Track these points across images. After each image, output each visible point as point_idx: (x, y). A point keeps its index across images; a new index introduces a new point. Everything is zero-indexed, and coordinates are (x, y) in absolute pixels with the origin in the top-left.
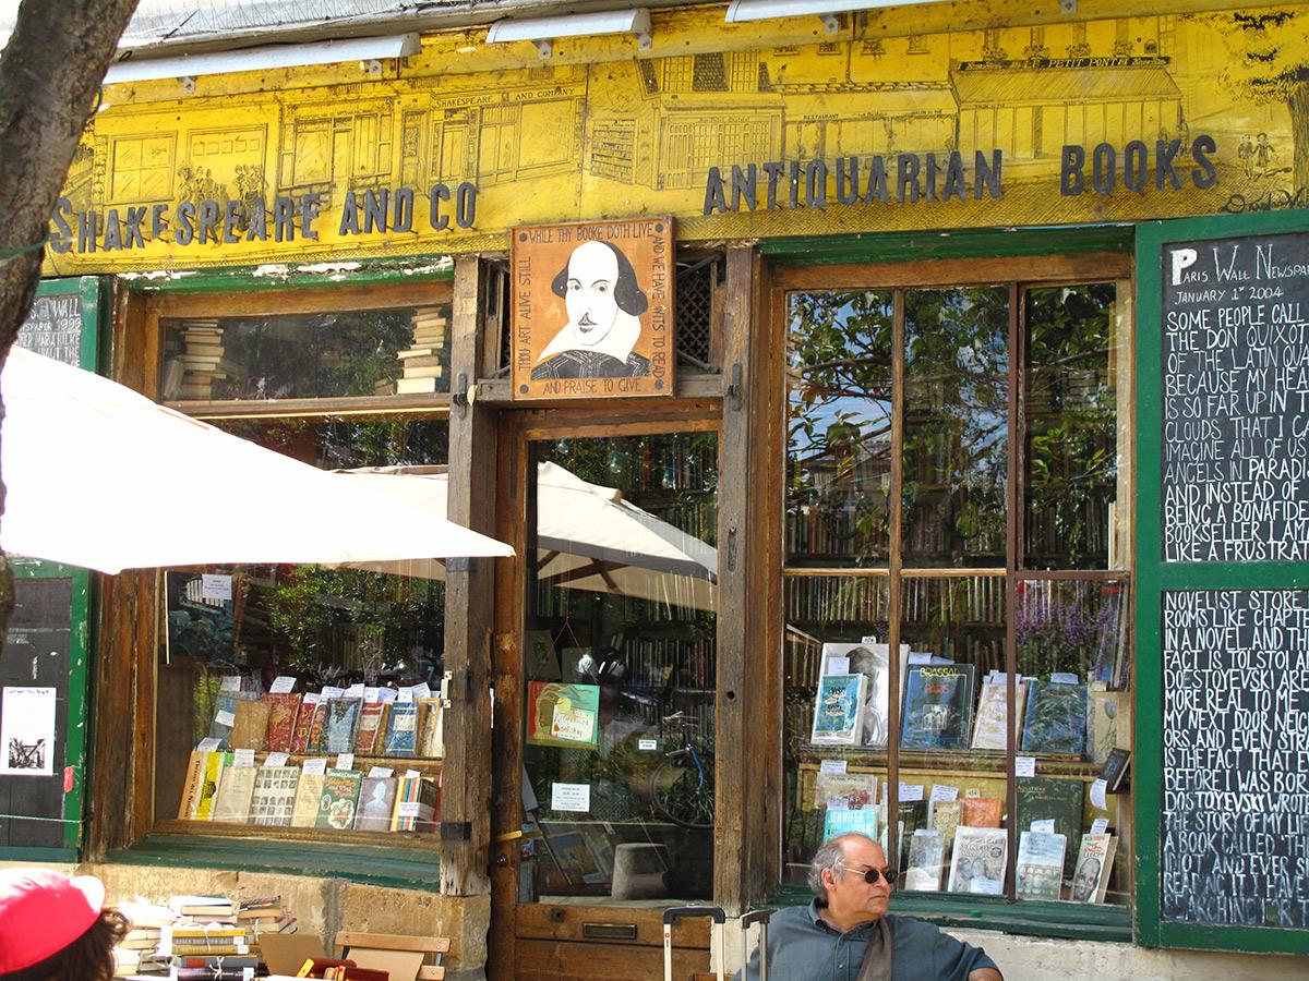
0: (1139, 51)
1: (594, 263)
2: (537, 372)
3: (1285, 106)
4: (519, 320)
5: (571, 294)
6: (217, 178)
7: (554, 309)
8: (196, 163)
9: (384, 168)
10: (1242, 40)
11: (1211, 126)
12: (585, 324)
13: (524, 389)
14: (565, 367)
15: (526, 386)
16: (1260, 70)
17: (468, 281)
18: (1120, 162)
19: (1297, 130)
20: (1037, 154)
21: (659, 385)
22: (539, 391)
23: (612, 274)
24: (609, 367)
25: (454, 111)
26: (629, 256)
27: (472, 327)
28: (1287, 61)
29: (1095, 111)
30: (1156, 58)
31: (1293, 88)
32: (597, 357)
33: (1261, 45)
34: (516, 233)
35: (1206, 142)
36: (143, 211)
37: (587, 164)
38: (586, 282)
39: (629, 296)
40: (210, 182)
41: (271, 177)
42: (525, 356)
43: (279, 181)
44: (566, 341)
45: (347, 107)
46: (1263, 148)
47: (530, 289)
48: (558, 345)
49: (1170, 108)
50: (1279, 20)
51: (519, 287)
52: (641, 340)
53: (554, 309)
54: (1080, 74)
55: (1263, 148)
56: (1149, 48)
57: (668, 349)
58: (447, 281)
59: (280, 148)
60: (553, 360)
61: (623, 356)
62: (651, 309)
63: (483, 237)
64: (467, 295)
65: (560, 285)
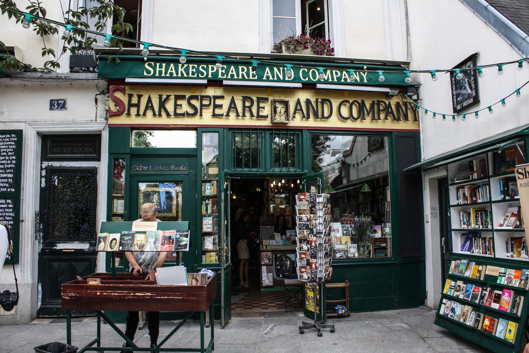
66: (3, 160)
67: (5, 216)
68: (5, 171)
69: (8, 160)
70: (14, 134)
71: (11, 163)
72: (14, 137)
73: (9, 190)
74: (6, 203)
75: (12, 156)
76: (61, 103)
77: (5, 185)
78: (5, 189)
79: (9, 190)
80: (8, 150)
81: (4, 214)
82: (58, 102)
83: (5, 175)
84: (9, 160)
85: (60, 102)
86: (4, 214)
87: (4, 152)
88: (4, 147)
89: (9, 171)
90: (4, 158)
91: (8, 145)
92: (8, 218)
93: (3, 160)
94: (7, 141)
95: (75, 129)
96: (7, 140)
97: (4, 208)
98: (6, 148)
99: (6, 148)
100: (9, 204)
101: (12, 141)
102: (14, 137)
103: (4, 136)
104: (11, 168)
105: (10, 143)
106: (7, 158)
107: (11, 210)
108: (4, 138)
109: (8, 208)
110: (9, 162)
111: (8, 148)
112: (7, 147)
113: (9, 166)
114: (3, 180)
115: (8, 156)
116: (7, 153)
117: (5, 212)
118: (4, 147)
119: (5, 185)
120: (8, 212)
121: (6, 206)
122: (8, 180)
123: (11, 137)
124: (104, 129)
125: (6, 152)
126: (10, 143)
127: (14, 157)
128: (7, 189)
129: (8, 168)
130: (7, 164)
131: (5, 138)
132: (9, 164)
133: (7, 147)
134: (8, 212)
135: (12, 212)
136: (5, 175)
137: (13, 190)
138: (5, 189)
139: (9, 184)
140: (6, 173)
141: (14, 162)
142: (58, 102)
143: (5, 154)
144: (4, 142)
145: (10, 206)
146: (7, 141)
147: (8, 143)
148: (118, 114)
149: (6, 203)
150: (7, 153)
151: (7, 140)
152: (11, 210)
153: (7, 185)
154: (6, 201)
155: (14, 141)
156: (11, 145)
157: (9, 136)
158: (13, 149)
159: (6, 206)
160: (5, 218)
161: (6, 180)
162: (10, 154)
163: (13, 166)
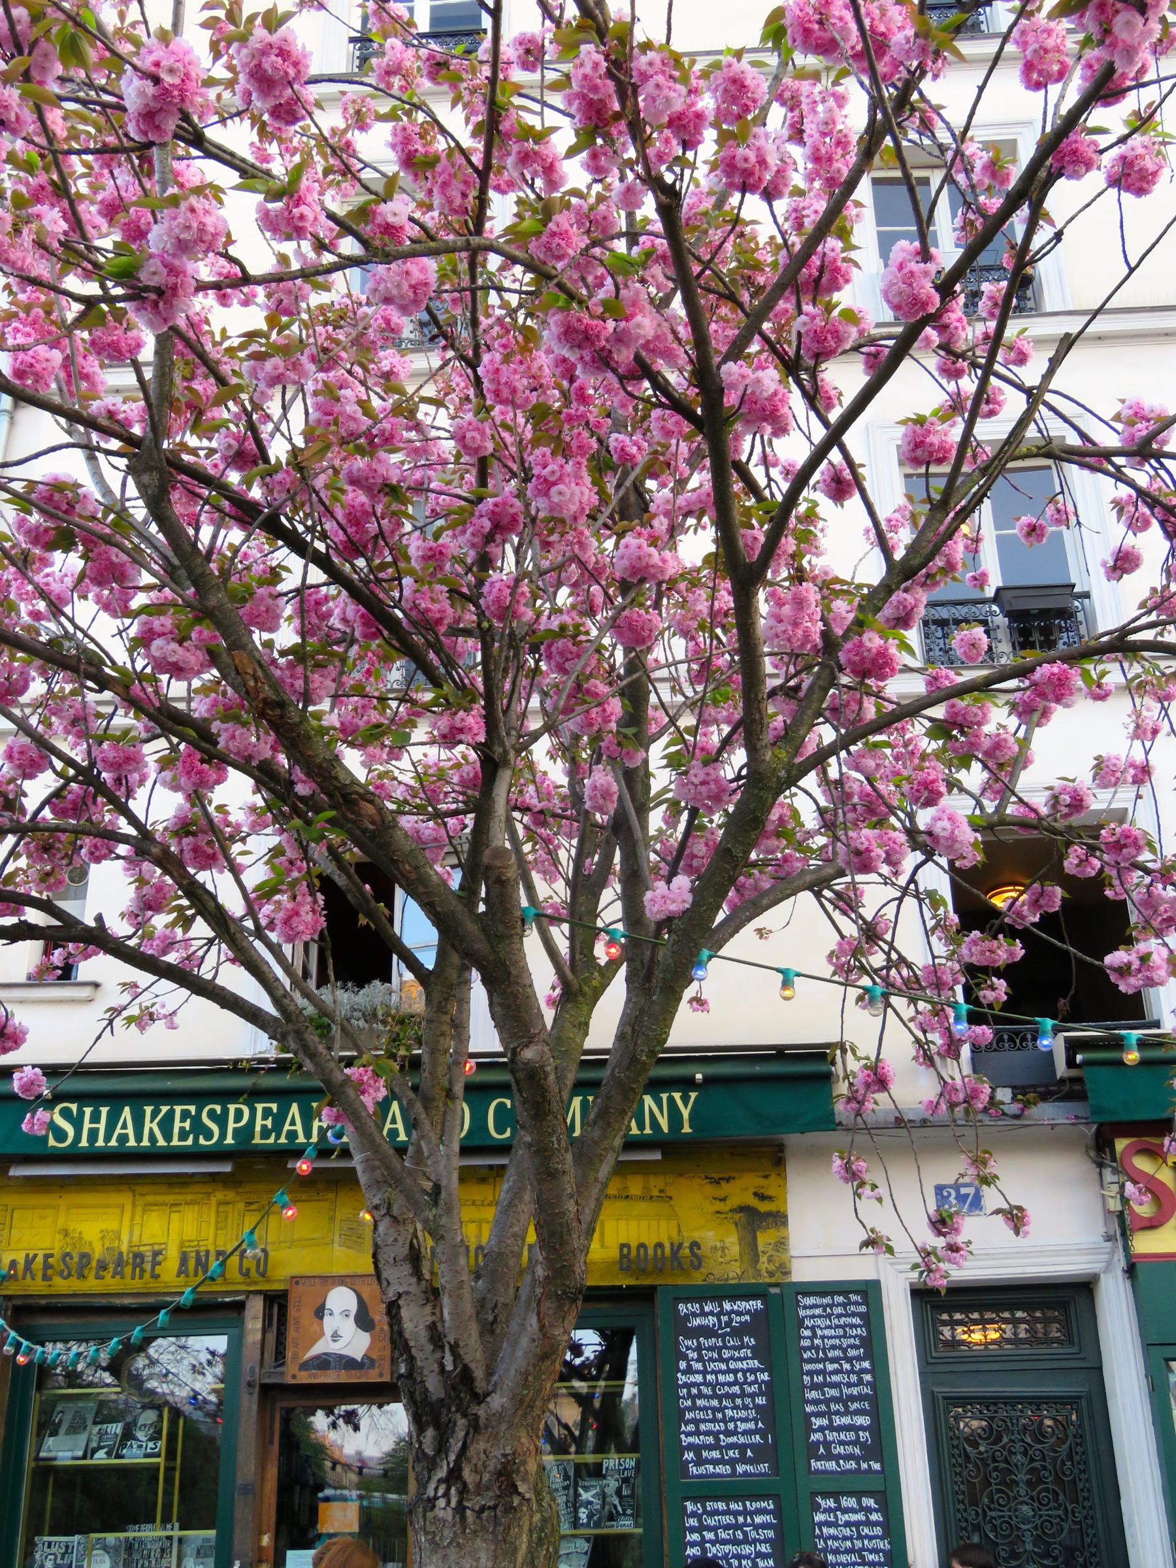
0: (655, 1193)
1: (341, 1300)
2: (304, 1366)
3: (733, 1227)
4: (291, 1333)
5: (327, 1319)
6: (87, 1236)
7: (316, 1327)
8: (72, 1226)
9: (203, 1236)
10: (710, 1190)
11: (697, 1236)
12: (336, 1336)
13: (294, 1377)
14: (323, 1362)
15: (294, 1375)
16: (720, 1206)
17: (256, 1307)
18: (651, 1252)
19: (741, 1239)
20: (602, 1246)
21: (381, 1375)
22: (304, 1378)
23: (353, 1306)
24: (349, 1363)
25: (250, 1203)
26: (364, 1296)
27: (259, 1336)
28: (733, 1202)
29: (633, 1223)
30: (665, 1198)
31: (737, 1216)
32: (341, 1357)
33: (720, 1193)
34: (296, 1280)
35: (695, 1245)
36: (35, 1256)
37: (337, 1238)
38: (336, 1312)
39: (363, 1320)
40: (81, 1238)
41: (125, 1238)
42: (295, 1356)
43: (130, 1241)
44: (322, 1347)
45: (179, 1197)
46: (723, 1248)
47: (298, 1313)
48: (318, 1349)
49: (673, 1224)
50: (728, 1180)
51: (292, 1312)
52: (370, 1348)
53: (316, 1327)
54: (624, 1203)
55: (723, 1248)
56: (661, 1191)
57: (387, 1353)
58: (239, 1307)
59: (132, 1219)
60: (317, 1357)
61: (358, 1357)
62: (377, 1328)
63: (269, 1281)
64: (255, 1318)
65: (320, 1312)
66: (836, 1372)
67: (863, 1549)
68: (846, 1407)
69: (848, 1373)
70: (856, 1292)
71: (860, 1382)
72: (856, 1303)
73: (864, 1466)
74: (862, 1509)
75: (859, 1359)
76: (968, 1195)
77: (849, 1449)
78: (852, 1465)
79: (864, 1466)
80: (845, 1342)
81: (858, 1544)
82: (958, 1192)
83: (846, 1420)
84: (852, 1372)
85: (963, 1191)
86: (858, 1544)
87: (834, 1347)
88: (832, 1332)
89: (854, 1406)
90: (836, 1366)
91: (843, 1327)
92: (871, 1557)
93: (836, 1372)
94: (839, 1316)
95: (1019, 1270)
96: (839, 1310)
97: (857, 1524)
98: (839, 1337)
99: (839, 1337)
100: (869, 1510)
101: (854, 1315)
102: (856, 1303)
103: (827, 1300)
104: (860, 1398)
105: (849, 1320)
106: (847, 1366)
107: (878, 1531)
108: (828, 1305)
109: (869, 1523)
110: (854, 1378)
111: (845, 1336)
112: (841, 1331)
113: (855, 1391)
114: (842, 1437)
115: (849, 1360)
116: (845, 1351)
117: (860, 1537)
118: (832, 1332)
119: (849, 1449)
120: (871, 1538)
121: (860, 1517)
122: (858, 1436)
123: (850, 1303)
124: (1107, 1270)
125: (840, 1347)
126: (849, 1320)
127: (866, 1364)
128: (858, 1464)
129: (852, 1398)
130: (849, 1385)
131: (831, 1306)
132: (854, 1385)
133: (841, 1331)
134: (871, 1538)
135: (882, 1538)
136: (846, 1420)
137: (877, 1466)
138: (852, 1465)
139: (863, 1446)
140: (847, 1412)
141: (868, 1377)
142: (958, 1192)
143: (838, 1353)
144: (829, 1316)
145: (875, 1517)
146: (839, 1316)
147: (843, 1320)
148: (1152, 1225)
149: (862, 1509)
150: (845, 1351)
151: (839, 1310)
152: (878, 1531)
153: (857, 1451)
154: (859, 1503)
155: (860, 1315)
156: (852, 1326)
157: (841, 1299)
158: (860, 1337)
159: (860, 1517)
160: (862, 1557)
161: (851, 1436)
162: (852, 1353)
163: (867, 1390)
